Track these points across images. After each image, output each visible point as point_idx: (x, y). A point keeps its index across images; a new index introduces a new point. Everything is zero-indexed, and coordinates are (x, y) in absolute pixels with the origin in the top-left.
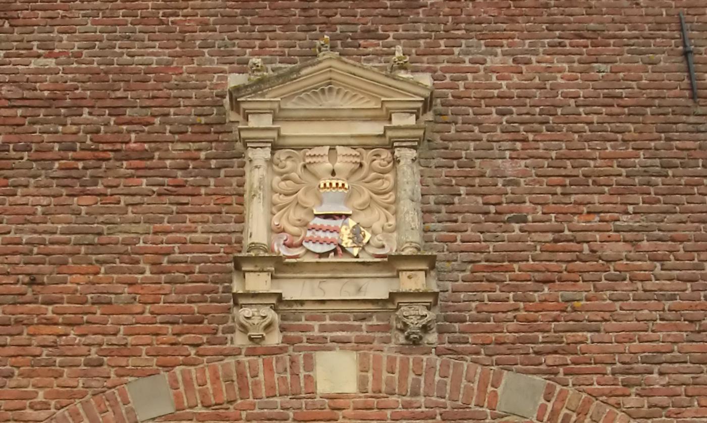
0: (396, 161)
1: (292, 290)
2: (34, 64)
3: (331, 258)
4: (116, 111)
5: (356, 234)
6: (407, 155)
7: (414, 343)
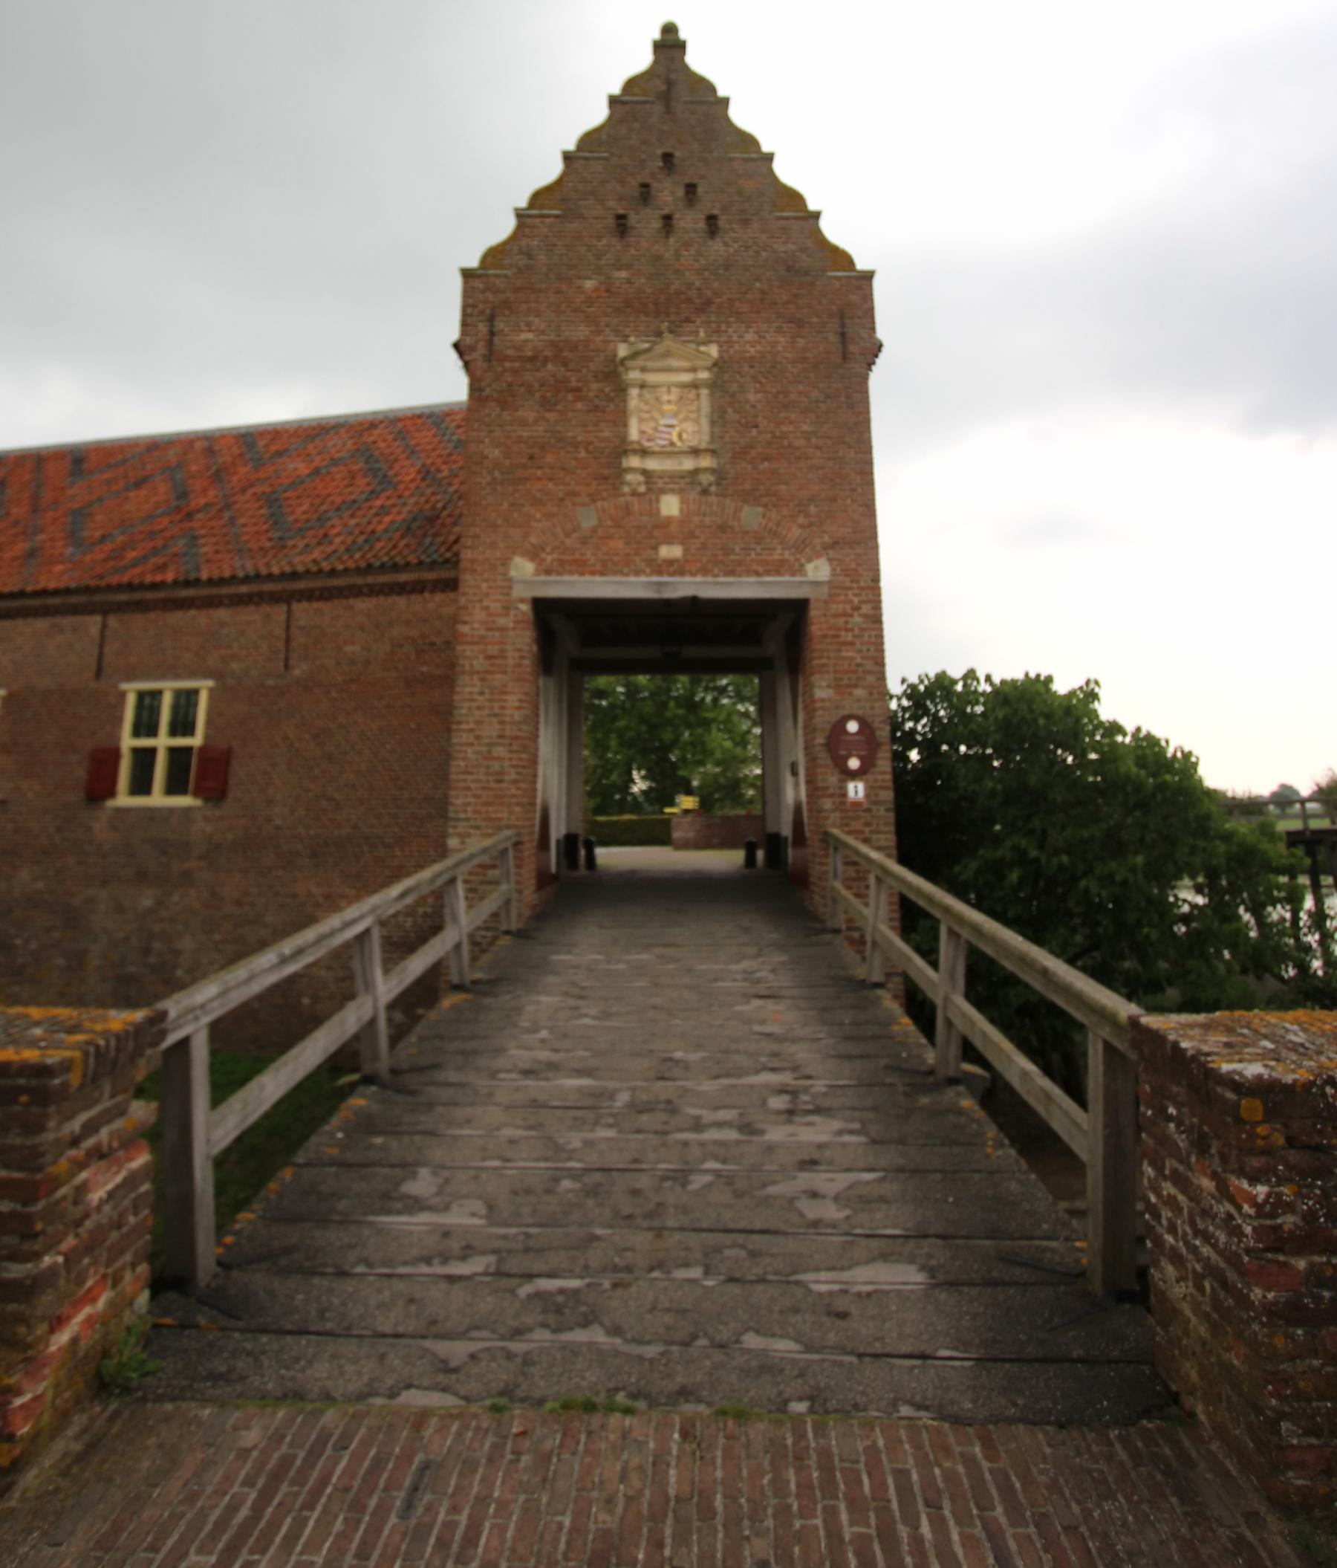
0: (698, 395)
1: (652, 464)
2: (525, 336)
3: (669, 449)
4: (565, 364)
5: (680, 436)
6: (704, 392)
7: (705, 492)
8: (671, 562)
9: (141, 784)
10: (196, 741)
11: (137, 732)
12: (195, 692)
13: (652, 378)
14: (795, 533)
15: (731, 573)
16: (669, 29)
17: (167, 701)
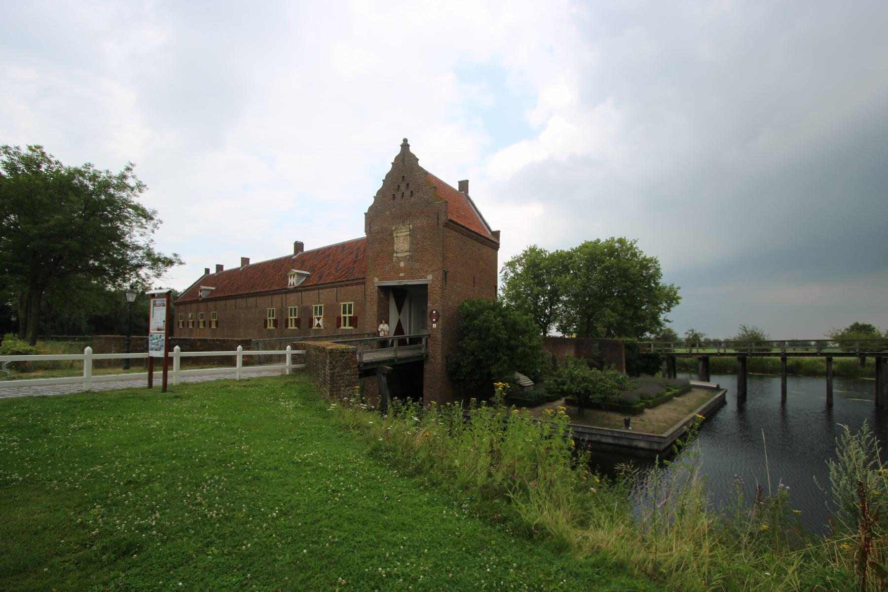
1: (399, 255)
8: (402, 277)
9: (345, 325)
10: (352, 315)
11: (343, 314)
12: (351, 305)
13: (399, 235)
14: (426, 268)
15: (413, 279)
16: (405, 140)
17: (347, 306)
